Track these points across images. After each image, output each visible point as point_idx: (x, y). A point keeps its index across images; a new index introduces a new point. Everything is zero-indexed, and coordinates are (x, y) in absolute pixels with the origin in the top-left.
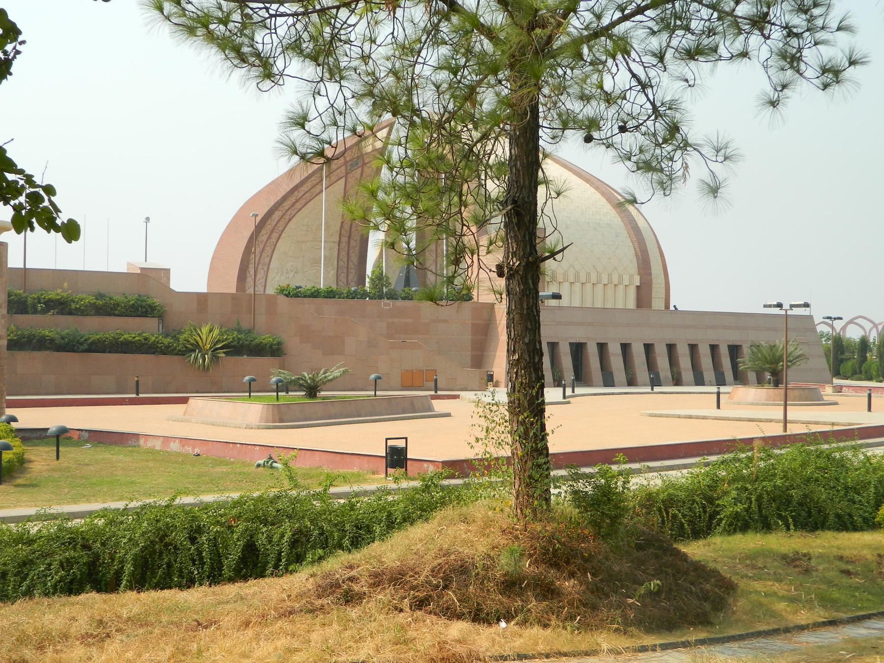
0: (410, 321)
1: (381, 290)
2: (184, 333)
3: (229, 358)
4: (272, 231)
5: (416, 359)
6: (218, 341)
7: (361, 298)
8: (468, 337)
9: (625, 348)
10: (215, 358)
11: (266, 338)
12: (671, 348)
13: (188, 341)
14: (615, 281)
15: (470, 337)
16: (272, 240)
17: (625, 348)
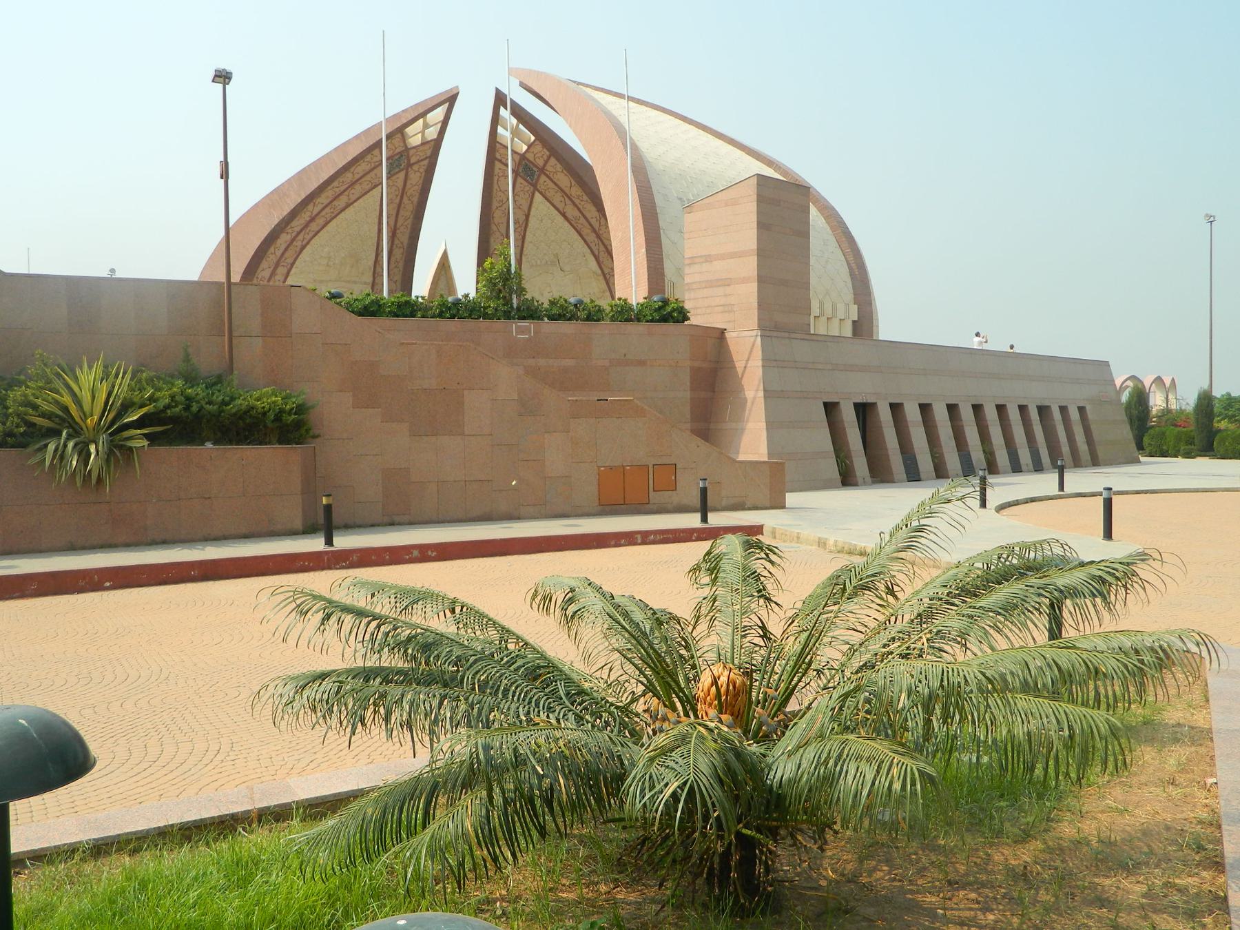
0: (569, 363)
1: (508, 302)
2: (20, 384)
3: (162, 451)
4: (277, 265)
5: (628, 443)
6: (126, 407)
7: (470, 316)
8: (683, 394)
9: (925, 408)
10: (119, 452)
11: (263, 397)
12: (977, 409)
13: (35, 407)
14: (829, 313)
15: (688, 394)
16: (277, 277)
17: (925, 408)
